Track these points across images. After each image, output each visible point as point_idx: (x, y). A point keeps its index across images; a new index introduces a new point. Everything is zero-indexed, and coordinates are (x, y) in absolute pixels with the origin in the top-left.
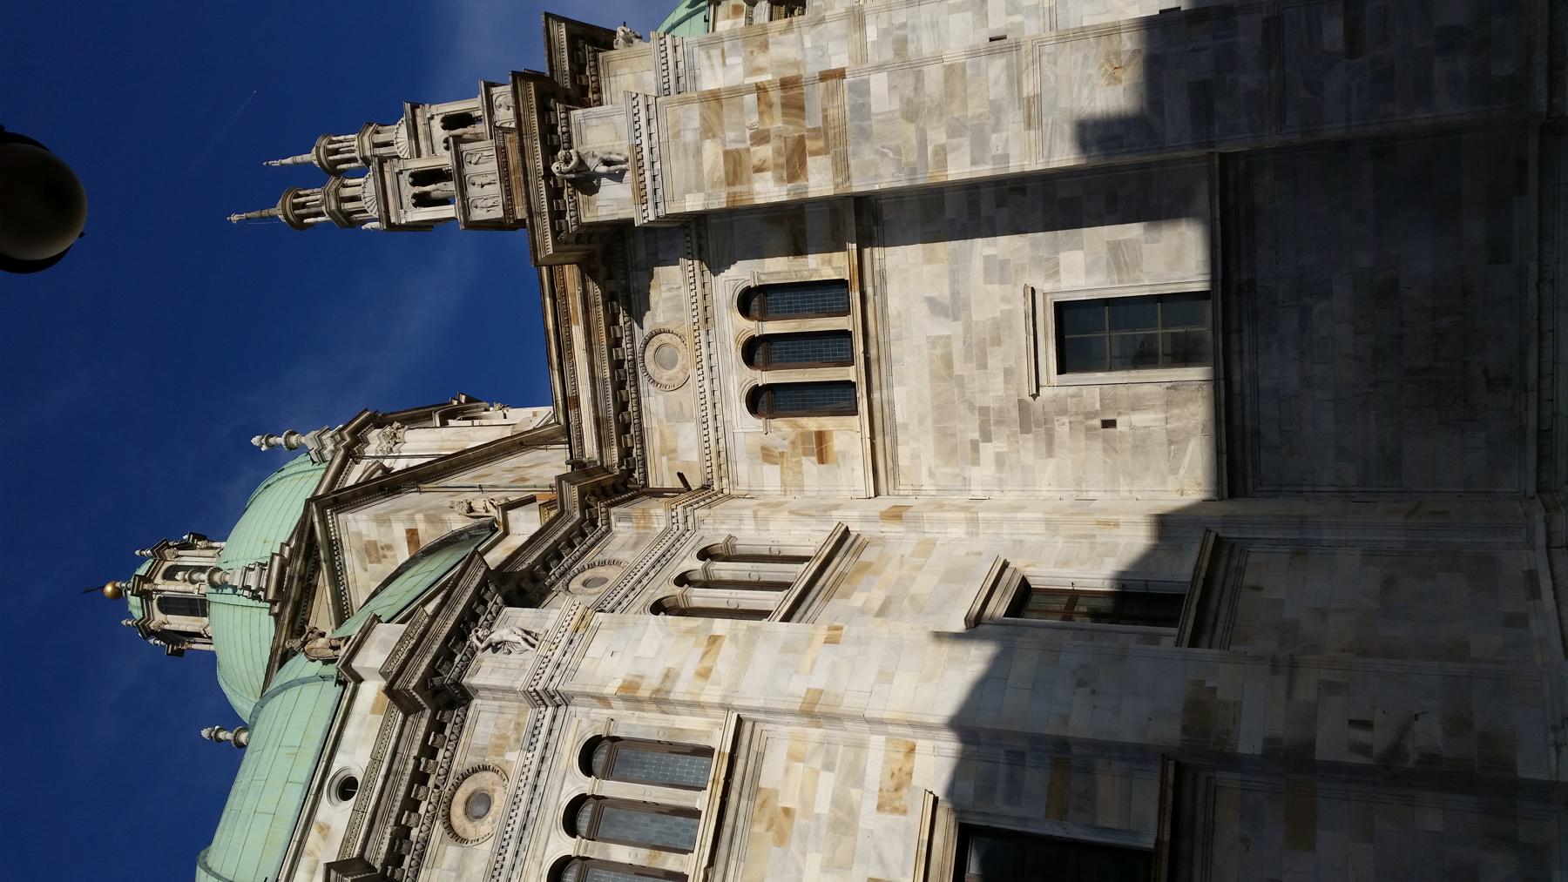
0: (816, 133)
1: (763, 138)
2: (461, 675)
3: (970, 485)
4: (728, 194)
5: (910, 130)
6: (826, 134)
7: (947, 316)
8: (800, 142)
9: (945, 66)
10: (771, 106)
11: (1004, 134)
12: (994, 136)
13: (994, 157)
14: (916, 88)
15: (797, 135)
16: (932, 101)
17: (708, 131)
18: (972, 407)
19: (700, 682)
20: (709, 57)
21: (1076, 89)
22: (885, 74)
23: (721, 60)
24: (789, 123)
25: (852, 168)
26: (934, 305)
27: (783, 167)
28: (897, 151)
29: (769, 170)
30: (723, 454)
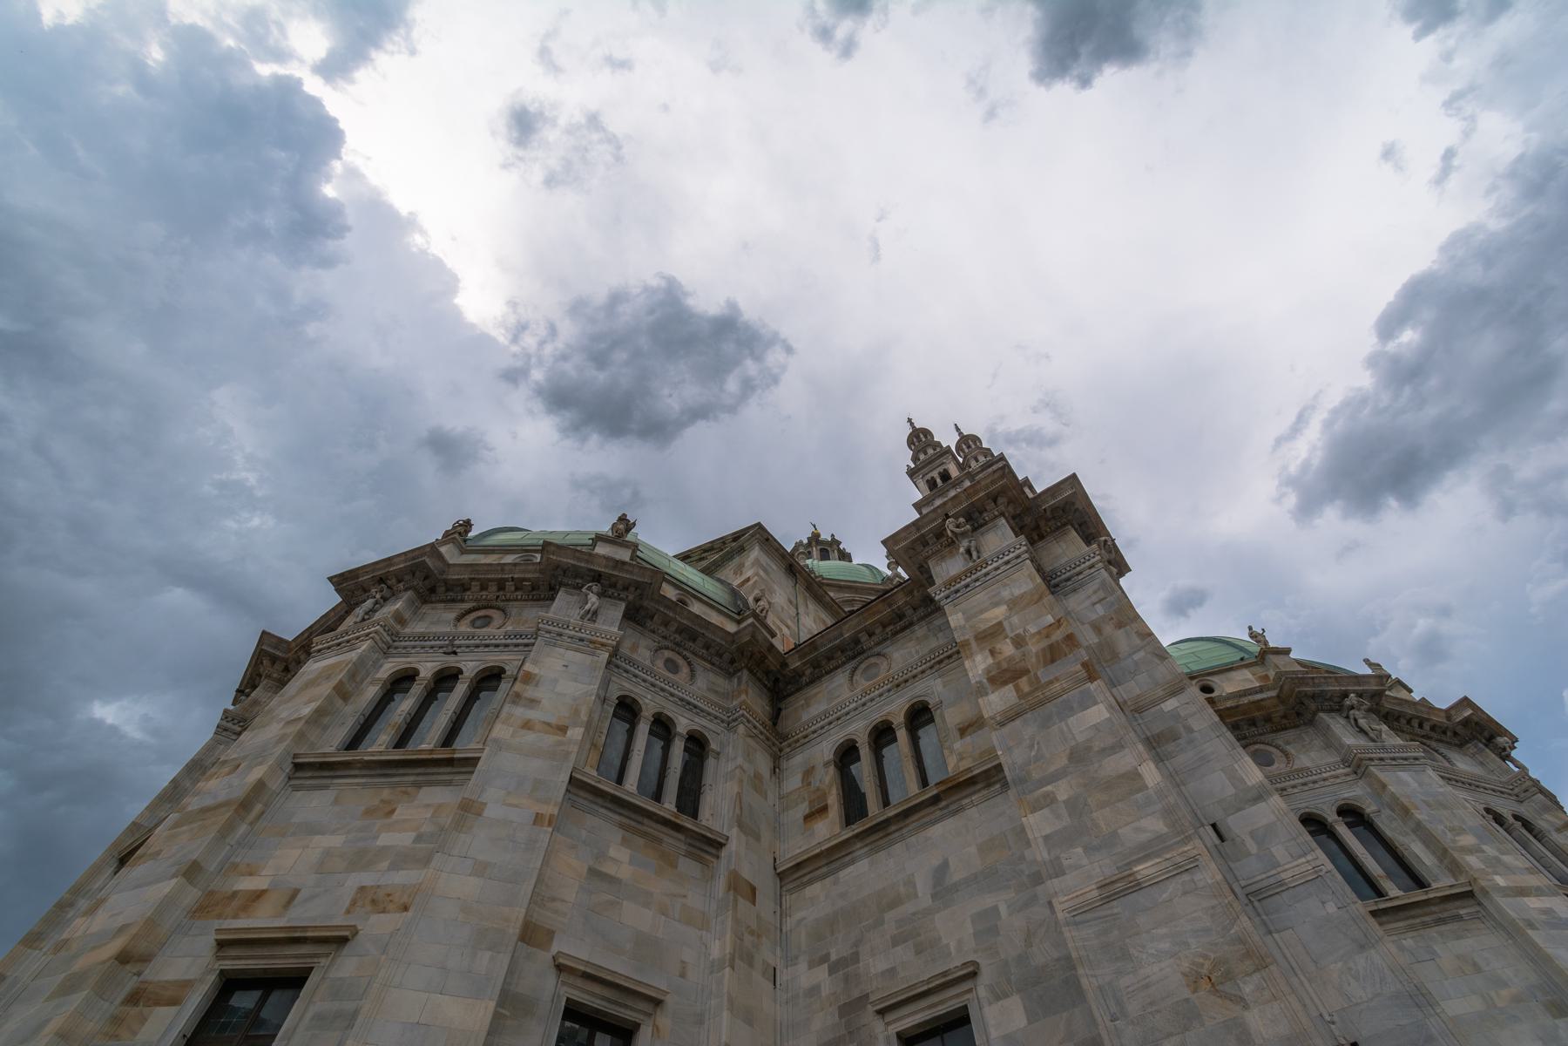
1: (1019, 644)
2: (566, 585)
3: (791, 965)
4: (968, 640)
5: (1064, 761)
6: (1036, 689)
8: (1025, 672)
9: (1137, 769)
11: (1085, 861)
12: (1079, 850)
13: (1058, 858)
14: (1104, 750)
16: (1096, 771)
17: (1013, 604)
18: (857, 944)
20: (1095, 592)
21: (1163, 931)
22: (1108, 715)
23: (1097, 600)
25: (1013, 724)
26: (942, 870)
29: (994, 660)
30: (807, 740)
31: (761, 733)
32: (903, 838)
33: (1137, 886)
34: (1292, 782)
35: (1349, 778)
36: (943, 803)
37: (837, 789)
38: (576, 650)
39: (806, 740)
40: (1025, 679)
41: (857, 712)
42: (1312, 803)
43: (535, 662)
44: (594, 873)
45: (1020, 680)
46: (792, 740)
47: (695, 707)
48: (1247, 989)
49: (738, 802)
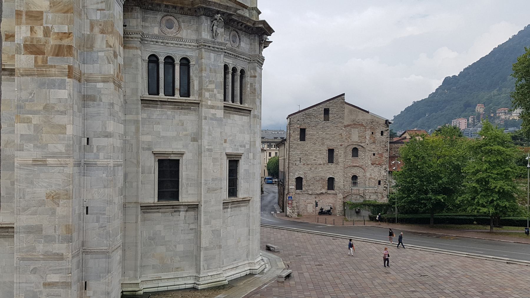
0: (45, 61)
1: (46, 33)
5: (41, 108)
6: (44, 66)
8: (43, 53)
9: (66, 125)
10: (61, 39)
11: (32, 150)
12: (32, 145)
14: (59, 111)
15: (46, 51)
21: (47, 180)
24: (52, 48)
25: (27, 77)
27: (31, 42)
28: (32, 100)
29: (31, 35)
33: (46, 165)
34: (173, 42)
35: (194, 48)
40: (41, 56)
42: (174, 53)
48: (61, 202)
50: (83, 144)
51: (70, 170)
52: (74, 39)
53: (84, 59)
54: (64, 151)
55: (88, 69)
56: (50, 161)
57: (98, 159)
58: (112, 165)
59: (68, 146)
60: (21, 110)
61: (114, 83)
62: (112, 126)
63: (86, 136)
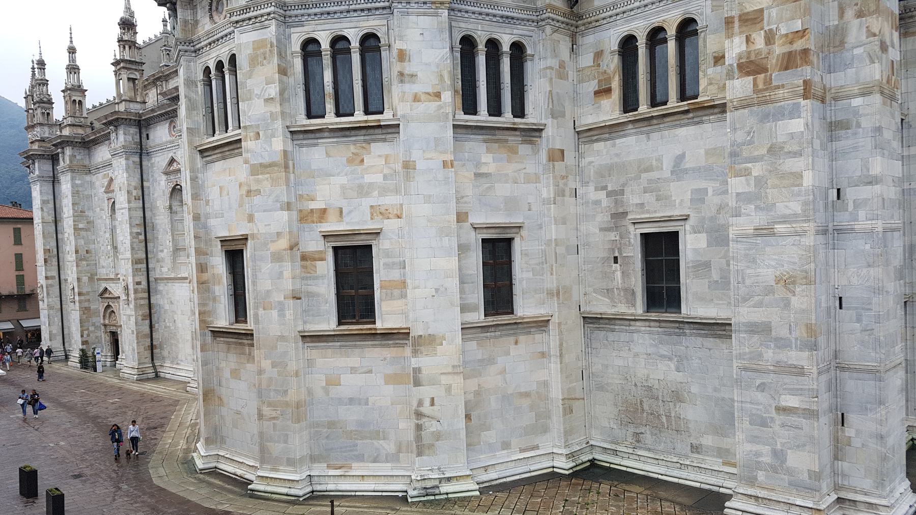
5: (764, 151)
7: (674, 167)
11: (753, 214)
12: (753, 207)
14: (790, 152)
19: (411, 98)
22: (802, 129)
25: (742, 111)
26: (681, 158)
28: (751, 143)
30: (598, 24)
31: (563, 23)
32: (660, 130)
36: (691, 115)
37: (619, 76)
38: (425, 14)
39: (596, 25)
41: (639, 11)
43: (401, 38)
44: (478, 175)
45: (759, 75)
46: (586, 20)
47: (513, 18)
49: (550, 100)
50: (830, 199)
51: (809, 240)
52: (812, 38)
53: (830, 66)
54: (800, 212)
55: (835, 80)
56: (780, 228)
57: (858, 220)
58: (880, 229)
59: (805, 203)
60: (737, 158)
61: (882, 93)
62: (877, 166)
63: (835, 186)
